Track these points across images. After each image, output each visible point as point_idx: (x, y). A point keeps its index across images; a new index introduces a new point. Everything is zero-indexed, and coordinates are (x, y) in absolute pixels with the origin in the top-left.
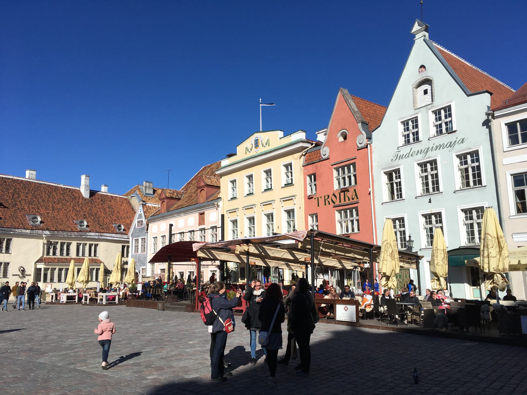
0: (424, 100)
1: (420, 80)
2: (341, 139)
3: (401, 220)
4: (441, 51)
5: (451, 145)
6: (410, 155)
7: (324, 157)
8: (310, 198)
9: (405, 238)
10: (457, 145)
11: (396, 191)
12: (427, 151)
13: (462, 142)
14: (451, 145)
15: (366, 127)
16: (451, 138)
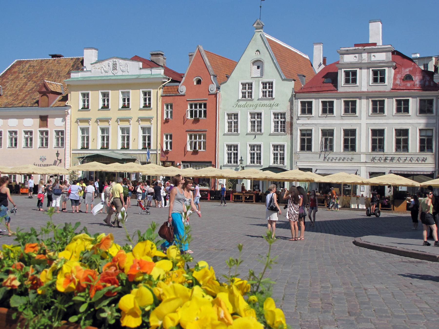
0: (256, 72)
1: (256, 59)
2: (195, 84)
3: (236, 147)
4: (269, 40)
5: (271, 106)
6: (244, 106)
7: (181, 93)
8: (167, 121)
9: (237, 157)
10: (274, 107)
11: (233, 126)
12: (256, 106)
13: (277, 106)
14: (271, 106)
15: (216, 78)
16: (272, 102)
